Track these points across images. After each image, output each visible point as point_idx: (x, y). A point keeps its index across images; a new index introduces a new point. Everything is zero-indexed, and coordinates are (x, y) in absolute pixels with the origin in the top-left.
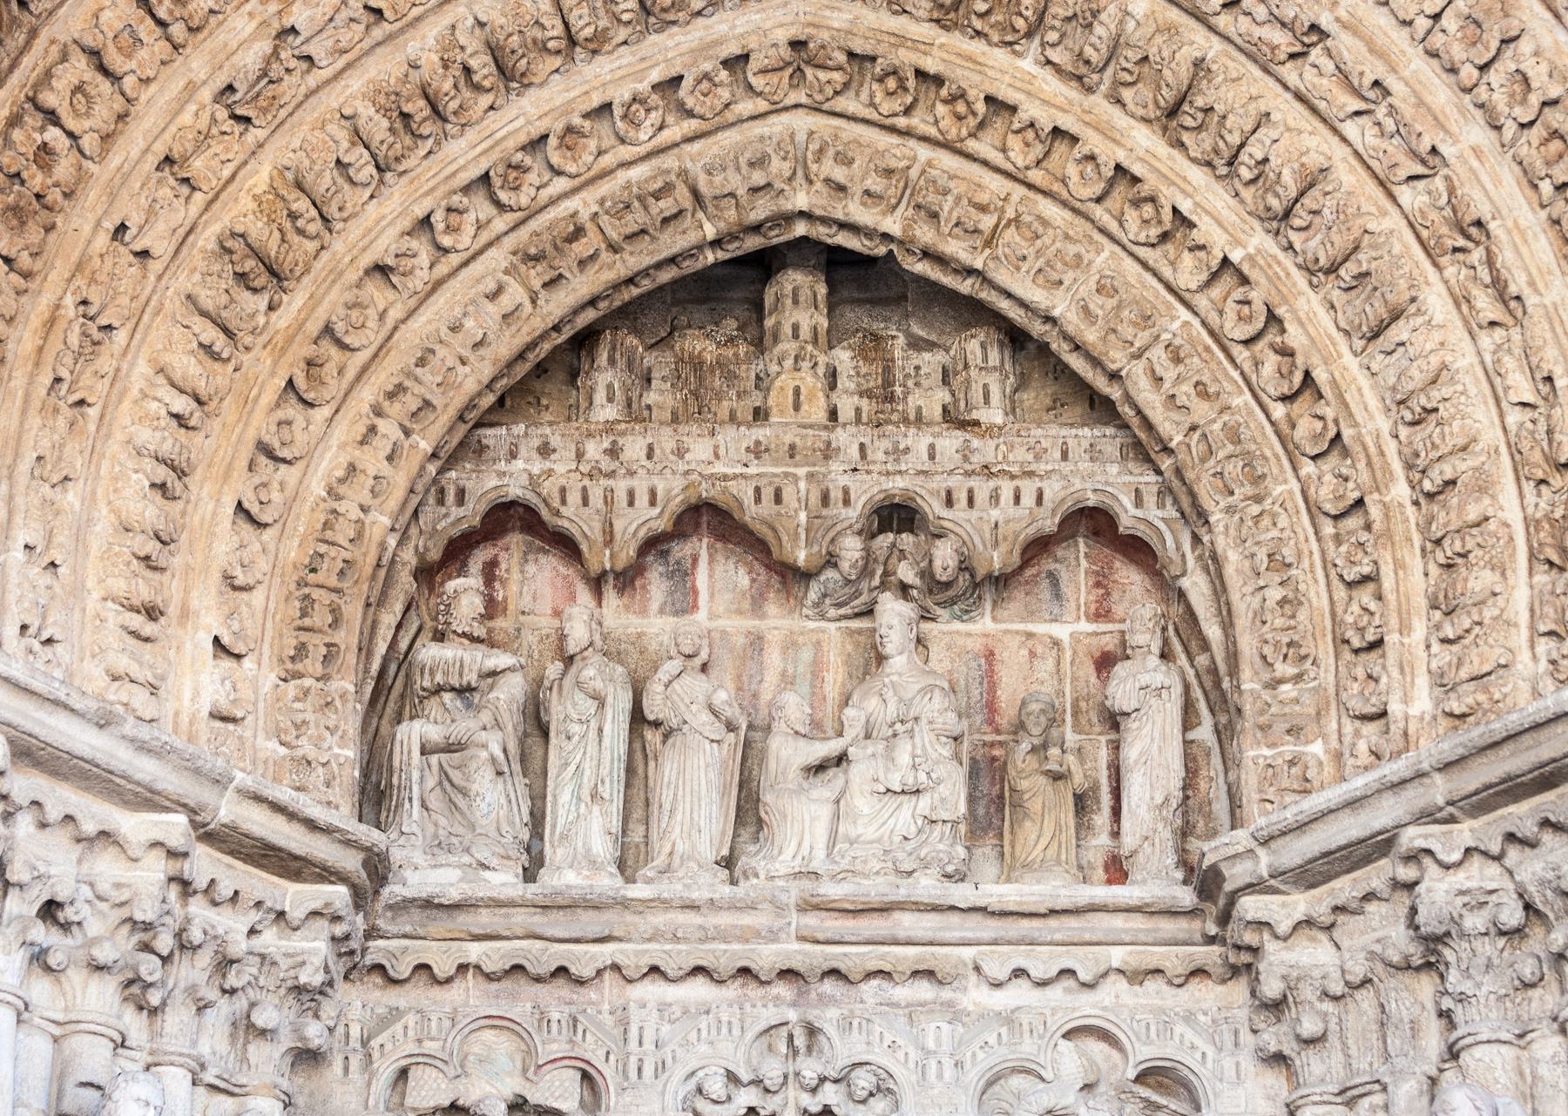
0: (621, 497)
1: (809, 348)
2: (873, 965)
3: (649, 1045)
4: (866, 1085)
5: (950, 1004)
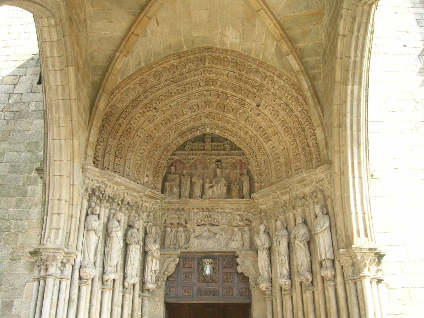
0: (189, 159)
2: (216, 208)
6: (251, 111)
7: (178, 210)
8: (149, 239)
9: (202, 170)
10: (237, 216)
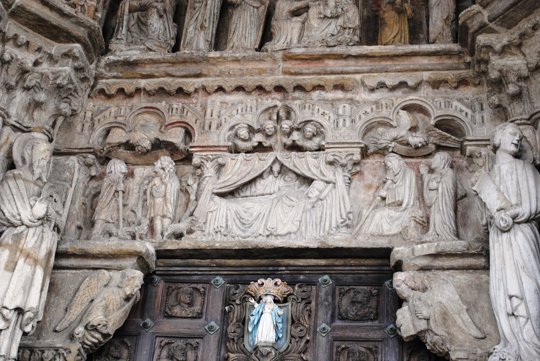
2: (316, 82)
3: (214, 116)
4: (311, 130)
5: (351, 99)
7: (161, 92)
8: (12, 183)
10: (403, 113)
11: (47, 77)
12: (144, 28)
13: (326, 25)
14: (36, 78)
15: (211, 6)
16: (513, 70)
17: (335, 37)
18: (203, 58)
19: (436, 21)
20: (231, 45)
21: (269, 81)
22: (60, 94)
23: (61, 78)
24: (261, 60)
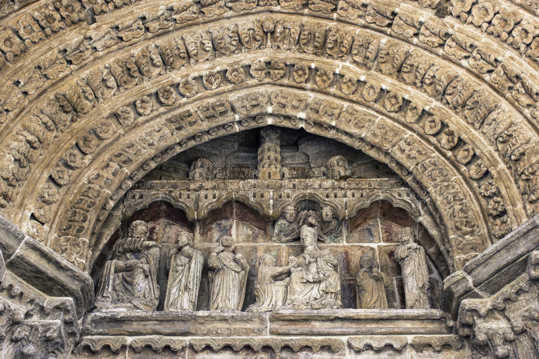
1: (274, 161)
2: (305, 343)
6: (416, 35)
9: (248, 241)
11: (37, 329)
12: (129, 287)
13: (309, 290)
14: (25, 330)
15: (194, 269)
16: (498, 334)
17: (318, 301)
18: (191, 316)
19: (412, 289)
20: (215, 306)
21: (257, 340)
22: (48, 348)
23: (51, 331)
24: (250, 320)
